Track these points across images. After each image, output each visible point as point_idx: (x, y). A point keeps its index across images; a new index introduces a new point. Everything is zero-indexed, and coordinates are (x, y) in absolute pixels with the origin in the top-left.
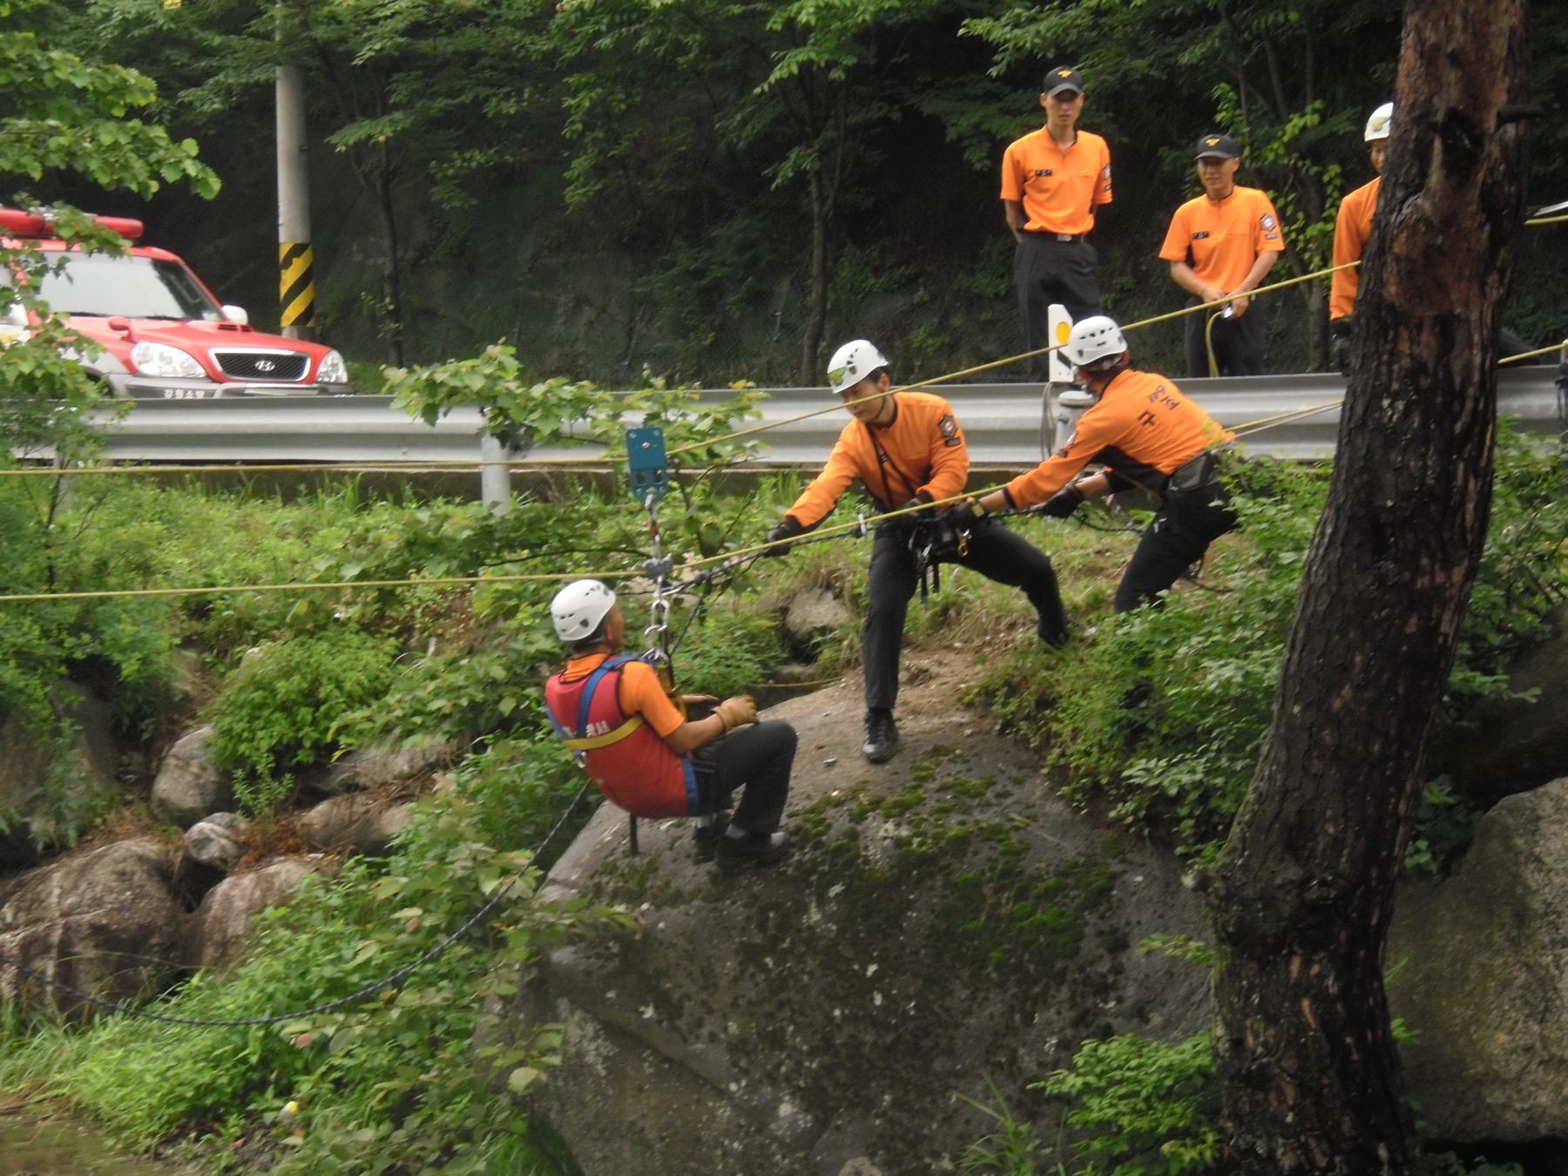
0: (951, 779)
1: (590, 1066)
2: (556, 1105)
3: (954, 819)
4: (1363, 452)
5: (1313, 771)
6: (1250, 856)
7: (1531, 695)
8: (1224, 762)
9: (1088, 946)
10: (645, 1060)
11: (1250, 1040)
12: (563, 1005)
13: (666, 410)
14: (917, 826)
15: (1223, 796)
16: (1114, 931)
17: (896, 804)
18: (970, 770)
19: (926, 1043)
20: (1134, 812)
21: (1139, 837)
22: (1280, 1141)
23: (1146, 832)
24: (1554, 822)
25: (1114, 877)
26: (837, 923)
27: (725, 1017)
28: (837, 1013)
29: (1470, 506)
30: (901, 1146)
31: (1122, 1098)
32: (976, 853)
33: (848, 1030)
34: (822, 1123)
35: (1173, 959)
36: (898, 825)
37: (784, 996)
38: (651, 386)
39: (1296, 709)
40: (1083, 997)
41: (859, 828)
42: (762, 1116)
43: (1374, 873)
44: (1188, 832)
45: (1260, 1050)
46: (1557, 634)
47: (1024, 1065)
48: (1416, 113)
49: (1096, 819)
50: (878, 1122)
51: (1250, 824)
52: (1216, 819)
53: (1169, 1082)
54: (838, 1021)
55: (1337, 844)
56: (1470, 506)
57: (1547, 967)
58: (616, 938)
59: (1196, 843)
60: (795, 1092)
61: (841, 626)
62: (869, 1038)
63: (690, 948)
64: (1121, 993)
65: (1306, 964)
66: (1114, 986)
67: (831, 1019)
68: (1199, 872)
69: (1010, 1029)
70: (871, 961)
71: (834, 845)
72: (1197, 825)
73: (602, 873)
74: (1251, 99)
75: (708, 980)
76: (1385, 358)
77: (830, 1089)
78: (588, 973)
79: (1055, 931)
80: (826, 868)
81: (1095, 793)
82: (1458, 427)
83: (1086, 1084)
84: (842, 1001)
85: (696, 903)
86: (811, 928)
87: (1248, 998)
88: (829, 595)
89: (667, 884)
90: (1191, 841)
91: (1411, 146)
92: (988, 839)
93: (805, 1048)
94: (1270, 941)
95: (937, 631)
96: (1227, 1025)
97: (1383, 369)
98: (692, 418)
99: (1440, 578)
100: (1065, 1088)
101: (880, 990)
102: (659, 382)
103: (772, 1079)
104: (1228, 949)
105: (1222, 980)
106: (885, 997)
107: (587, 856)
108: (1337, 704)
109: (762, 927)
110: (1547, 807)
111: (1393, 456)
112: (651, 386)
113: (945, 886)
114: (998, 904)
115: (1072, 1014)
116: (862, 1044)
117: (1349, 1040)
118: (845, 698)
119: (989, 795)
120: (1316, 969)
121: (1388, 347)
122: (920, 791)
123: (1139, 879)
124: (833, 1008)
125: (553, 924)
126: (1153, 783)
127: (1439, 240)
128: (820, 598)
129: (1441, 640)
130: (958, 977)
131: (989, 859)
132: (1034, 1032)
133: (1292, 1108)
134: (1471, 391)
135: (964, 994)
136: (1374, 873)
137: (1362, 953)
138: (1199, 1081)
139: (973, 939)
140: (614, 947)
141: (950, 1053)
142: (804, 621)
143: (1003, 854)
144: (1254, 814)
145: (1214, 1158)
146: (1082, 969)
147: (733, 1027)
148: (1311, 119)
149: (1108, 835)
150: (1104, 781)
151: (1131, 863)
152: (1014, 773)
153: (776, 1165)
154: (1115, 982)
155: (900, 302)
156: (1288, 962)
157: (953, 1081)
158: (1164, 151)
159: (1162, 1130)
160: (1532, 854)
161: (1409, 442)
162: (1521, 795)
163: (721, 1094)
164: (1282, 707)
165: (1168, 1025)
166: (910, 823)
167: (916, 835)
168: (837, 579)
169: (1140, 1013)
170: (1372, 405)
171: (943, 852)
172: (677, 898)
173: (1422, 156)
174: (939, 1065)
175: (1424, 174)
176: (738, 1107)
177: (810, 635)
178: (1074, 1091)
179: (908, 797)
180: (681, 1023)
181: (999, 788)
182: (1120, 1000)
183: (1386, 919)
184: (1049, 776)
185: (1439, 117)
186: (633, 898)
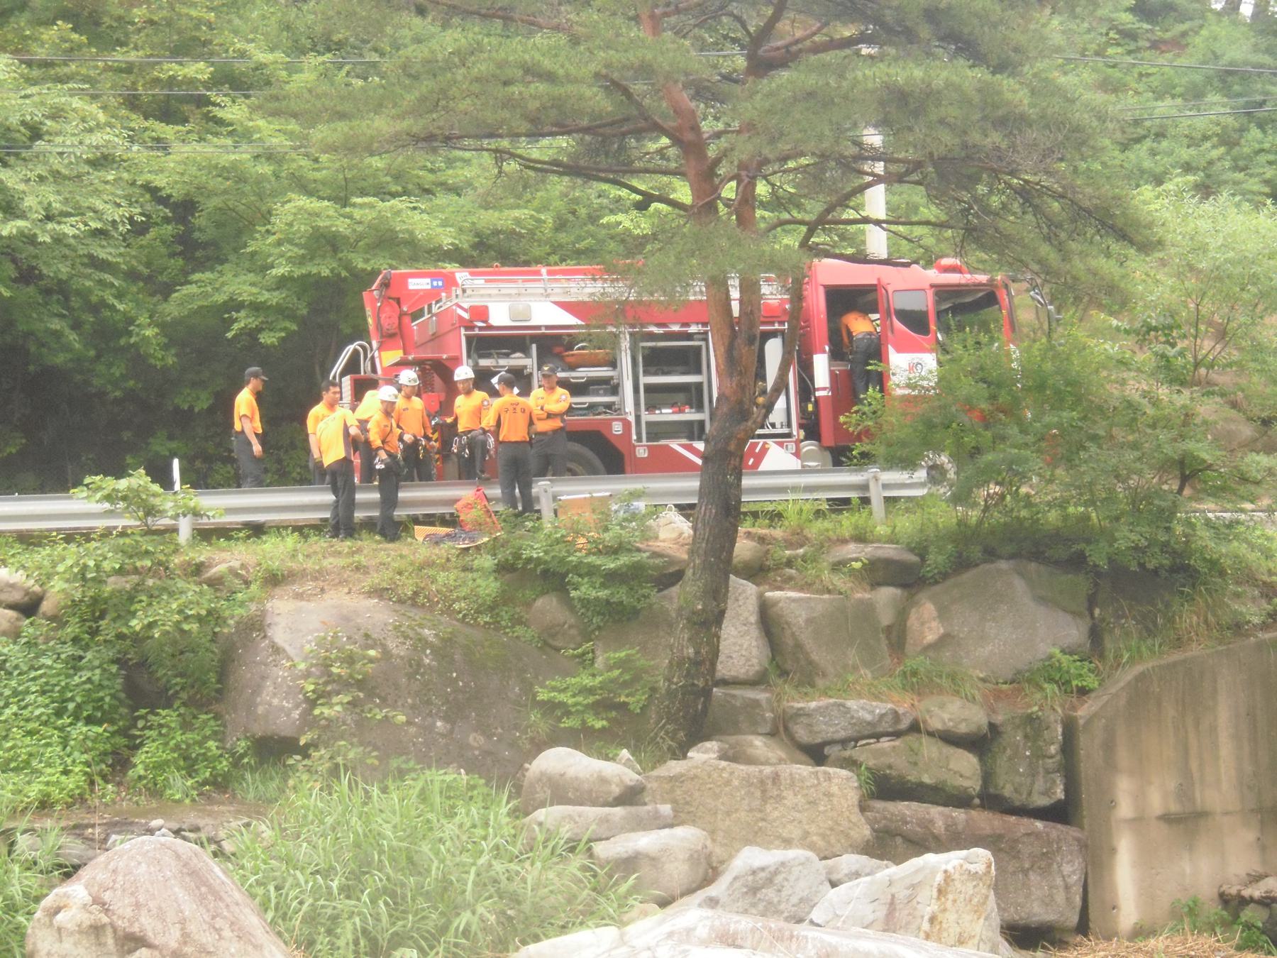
62: (460, 696)
75: (397, 686)
103: (430, 714)
109: (411, 666)
147: (410, 701)
174: (486, 701)
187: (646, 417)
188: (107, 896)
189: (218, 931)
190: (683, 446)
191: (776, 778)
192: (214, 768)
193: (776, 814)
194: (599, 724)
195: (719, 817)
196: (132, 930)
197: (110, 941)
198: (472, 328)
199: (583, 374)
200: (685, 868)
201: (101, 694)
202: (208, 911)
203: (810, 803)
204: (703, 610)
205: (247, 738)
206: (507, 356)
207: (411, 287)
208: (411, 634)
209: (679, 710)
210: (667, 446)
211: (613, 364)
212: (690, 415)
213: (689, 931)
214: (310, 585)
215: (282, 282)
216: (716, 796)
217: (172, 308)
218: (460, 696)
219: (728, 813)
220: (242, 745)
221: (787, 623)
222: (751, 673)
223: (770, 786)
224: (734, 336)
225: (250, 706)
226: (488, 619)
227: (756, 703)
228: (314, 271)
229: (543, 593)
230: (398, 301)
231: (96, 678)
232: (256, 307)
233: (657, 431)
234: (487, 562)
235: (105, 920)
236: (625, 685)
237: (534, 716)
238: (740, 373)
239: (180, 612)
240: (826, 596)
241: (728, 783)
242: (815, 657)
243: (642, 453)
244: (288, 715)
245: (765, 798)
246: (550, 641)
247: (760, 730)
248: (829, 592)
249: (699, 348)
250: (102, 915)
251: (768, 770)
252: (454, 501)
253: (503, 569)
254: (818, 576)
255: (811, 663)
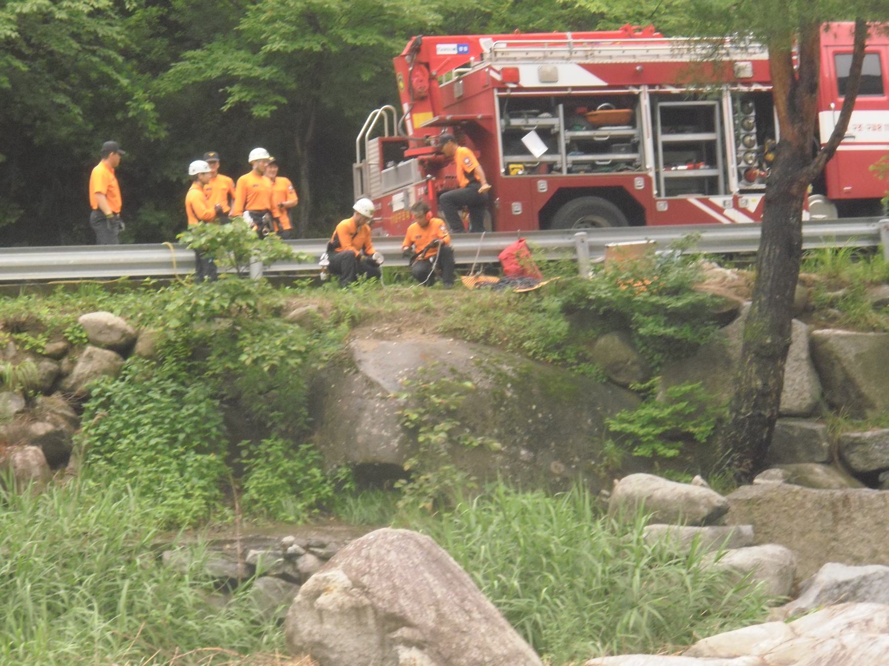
42: (515, 457)
62: (541, 427)
75: (484, 417)
103: (514, 443)
109: (495, 399)
187: (664, 173)
188: (365, 580)
189: (468, 612)
190: (700, 200)
191: (846, 500)
192: (318, 492)
193: (846, 534)
194: (671, 453)
195: (795, 537)
196: (392, 611)
197: (371, 622)
198: (504, 89)
199: (606, 132)
200: (775, 582)
201: (207, 426)
202: (457, 594)
203: (878, 523)
204: (771, 344)
205: (347, 465)
206: (536, 115)
207: (439, 52)
208: (492, 369)
209: (745, 440)
210: (685, 202)
211: (632, 121)
212: (704, 171)
213: (868, 622)
214: (386, 327)
215: (272, 58)
216: (791, 518)
217: (166, 84)
219: (803, 534)
220: (343, 473)
221: (837, 358)
222: (804, 406)
223: (840, 508)
224: (795, 85)
225: (350, 436)
226: (556, 357)
227: (814, 434)
228: (306, 46)
229: (603, 333)
230: (427, 65)
231: (203, 411)
232: (249, 82)
233: (675, 186)
234: (554, 303)
235: (366, 601)
236: (690, 417)
237: (610, 445)
238: (802, 120)
239: (284, 347)
240: (871, 334)
241: (801, 505)
242: (865, 390)
243: (662, 206)
244: (388, 443)
245: (836, 521)
246: (613, 377)
247: (817, 459)
248: (874, 329)
249: (711, 109)
250: (363, 597)
251: (839, 493)
252: (498, 252)
253: (568, 310)
254: (862, 316)
255: (860, 396)
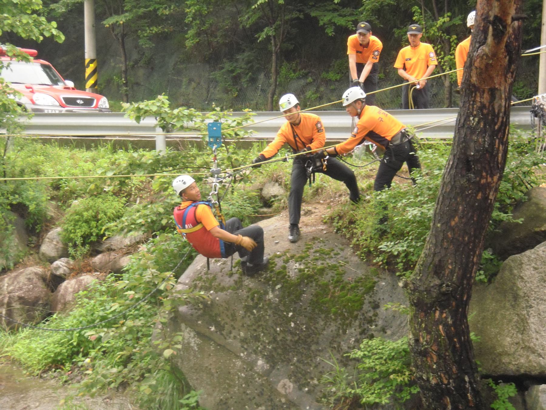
0: (319, 249)
1: (192, 347)
2: (180, 361)
3: (319, 263)
4: (463, 136)
5: (445, 246)
6: (422, 276)
7: (520, 221)
8: (414, 243)
9: (366, 307)
10: (211, 345)
11: (421, 340)
12: (183, 326)
13: (220, 119)
14: (307, 265)
15: (413, 255)
16: (375, 301)
17: (299, 257)
18: (325, 245)
19: (309, 340)
20: (382, 261)
21: (384, 269)
22: (431, 374)
23: (386, 267)
24: (527, 265)
25: (375, 283)
26: (278, 298)
27: (239, 330)
28: (278, 329)
29: (500, 155)
30: (300, 375)
31: (377, 359)
32: (327, 274)
33: (282, 335)
34: (273, 367)
35: (395, 311)
36: (300, 264)
37: (260, 323)
38: (215, 110)
39: (439, 225)
40: (364, 324)
41: (286, 265)
42: (251, 365)
43: (465, 282)
44: (401, 267)
45: (425, 343)
46: (530, 199)
47: (342, 348)
48: (483, 17)
49: (369, 263)
50: (292, 367)
51: (422, 265)
52: (410, 263)
53: (393, 354)
54: (278, 332)
55: (452, 272)
56: (500, 155)
57: (524, 315)
58: (201, 303)
59: (403, 271)
60: (263, 356)
61: (281, 195)
62: (289, 338)
63: (227, 306)
64: (377, 323)
65: (441, 313)
66: (375, 321)
67: (276, 331)
68: (405, 281)
69: (338, 335)
70: (290, 311)
71: (278, 271)
72: (404, 265)
73: (197, 280)
74: (426, 12)
75: (234, 317)
76: (471, 103)
77: (275, 356)
78: (192, 315)
79: (354, 301)
80: (275, 279)
81: (369, 253)
82: (496, 127)
83: (365, 355)
84: (280, 325)
85: (230, 291)
86: (269, 300)
87: (421, 325)
88: (277, 184)
89: (220, 284)
90: (402, 270)
91: (482, 29)
92: (331, 269)
93: (267, 341)
94: (429, 305)
95: (314, 197)
96: (414, 334)
97: (471, 107)
98: (230, 122)
99: (489, 180)
100: (357, 356)
101: (293, 322)
102: (218, 109)
103: (255, 352)
104: (414, 308)
105: (412, 319)
106: (295, 324)
107: (192, 274)
108: (453, 223)
109: (252, 299)
110: (525, 260)
111: (474, 137)
112: (215, 110)
113: (316, 286)
114: (335, 292)
115: (360, 330)
116: (287, 340)
117: (455, 340)
118: (282, 220)
119: (332, 254)
120: (444, 315)
121: (473, 99)
122: (308, 253)
123: (384, 284)
124: (277, 327)
125: (180, 298)
126: (389, 250)
127: (491, 62)
128: (274, 185)
129: (489, 201)
130: (320, 317)
131: (332, 277)
132: (346, 337)
133: (435, 363)
134: (501, 115)
135: (322, 323)
136: (465, 282)
137: (460, 310)
138: (403, 353)
139: (325, 304)
140: (201, 306)
141: (317, 343)
142: (268, 193)
143: (337, 274)
144: (424, 261)
145: (408, 380)
146: (363, 314)
147: (242, 334)
148: (446, 19)
149: (373, 268)
150: (372, 249)
151: (381, 278)
152: (341, 246)
153: (256, 381)
154: (375, 319)
155: (302, 82)
156: (435, 312)
157: (318, 353)
158: (395, 30)
159: (390, 370)
160: (520, 276)
161: (479, 132)
162: (516, 255)
163: (238, 357)
164: (434, 224)
165: (393, 334)
166: (304, 263)
167: (307, 268)
168: (280, 178)
169: (384, 330)
170: (467, 119)
171: (316, 274)
172: (223, 289)
173: (485, 32)
174: (313, 347)
175: (486, 38)
176: (244, 362)
177: (270, 198)
178: (360, 357)
179: (303, 255)
180: (224, 333)
181: (335, 252)
182: (376, 325)
183: (469, 297)
184: (353, 248)
185: (491, 19)
186: (207, 289)
218: (289, 338)
